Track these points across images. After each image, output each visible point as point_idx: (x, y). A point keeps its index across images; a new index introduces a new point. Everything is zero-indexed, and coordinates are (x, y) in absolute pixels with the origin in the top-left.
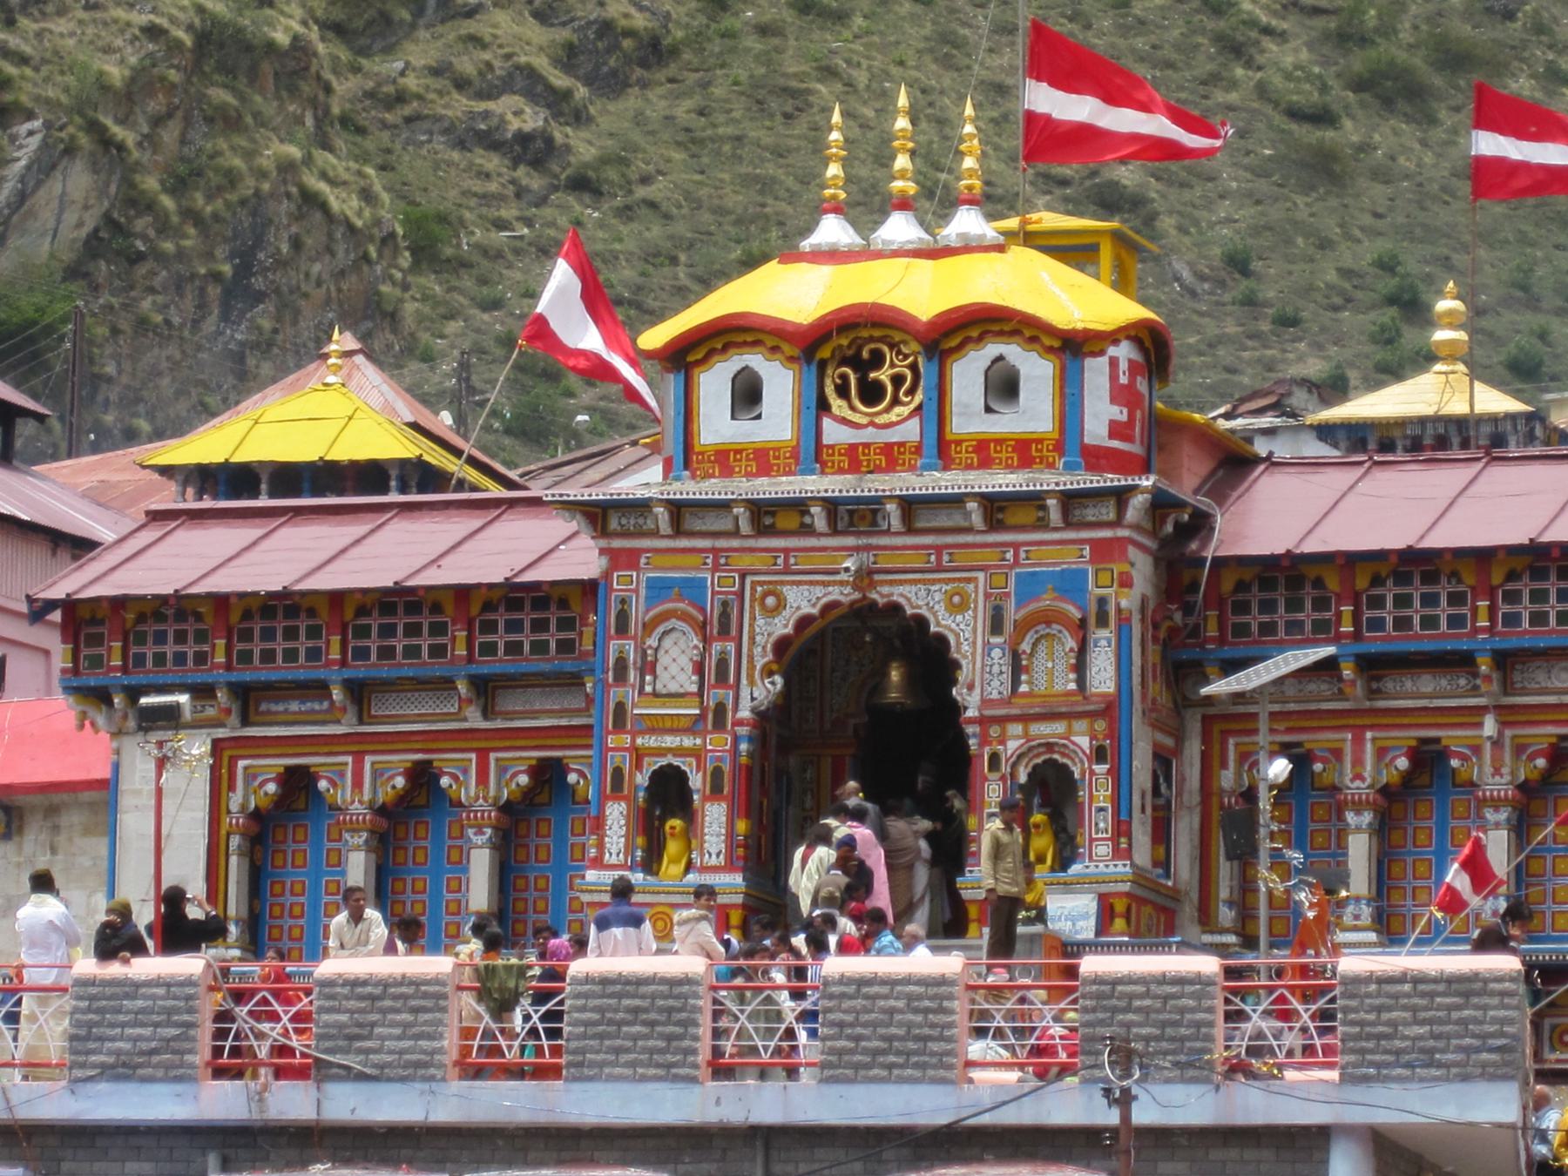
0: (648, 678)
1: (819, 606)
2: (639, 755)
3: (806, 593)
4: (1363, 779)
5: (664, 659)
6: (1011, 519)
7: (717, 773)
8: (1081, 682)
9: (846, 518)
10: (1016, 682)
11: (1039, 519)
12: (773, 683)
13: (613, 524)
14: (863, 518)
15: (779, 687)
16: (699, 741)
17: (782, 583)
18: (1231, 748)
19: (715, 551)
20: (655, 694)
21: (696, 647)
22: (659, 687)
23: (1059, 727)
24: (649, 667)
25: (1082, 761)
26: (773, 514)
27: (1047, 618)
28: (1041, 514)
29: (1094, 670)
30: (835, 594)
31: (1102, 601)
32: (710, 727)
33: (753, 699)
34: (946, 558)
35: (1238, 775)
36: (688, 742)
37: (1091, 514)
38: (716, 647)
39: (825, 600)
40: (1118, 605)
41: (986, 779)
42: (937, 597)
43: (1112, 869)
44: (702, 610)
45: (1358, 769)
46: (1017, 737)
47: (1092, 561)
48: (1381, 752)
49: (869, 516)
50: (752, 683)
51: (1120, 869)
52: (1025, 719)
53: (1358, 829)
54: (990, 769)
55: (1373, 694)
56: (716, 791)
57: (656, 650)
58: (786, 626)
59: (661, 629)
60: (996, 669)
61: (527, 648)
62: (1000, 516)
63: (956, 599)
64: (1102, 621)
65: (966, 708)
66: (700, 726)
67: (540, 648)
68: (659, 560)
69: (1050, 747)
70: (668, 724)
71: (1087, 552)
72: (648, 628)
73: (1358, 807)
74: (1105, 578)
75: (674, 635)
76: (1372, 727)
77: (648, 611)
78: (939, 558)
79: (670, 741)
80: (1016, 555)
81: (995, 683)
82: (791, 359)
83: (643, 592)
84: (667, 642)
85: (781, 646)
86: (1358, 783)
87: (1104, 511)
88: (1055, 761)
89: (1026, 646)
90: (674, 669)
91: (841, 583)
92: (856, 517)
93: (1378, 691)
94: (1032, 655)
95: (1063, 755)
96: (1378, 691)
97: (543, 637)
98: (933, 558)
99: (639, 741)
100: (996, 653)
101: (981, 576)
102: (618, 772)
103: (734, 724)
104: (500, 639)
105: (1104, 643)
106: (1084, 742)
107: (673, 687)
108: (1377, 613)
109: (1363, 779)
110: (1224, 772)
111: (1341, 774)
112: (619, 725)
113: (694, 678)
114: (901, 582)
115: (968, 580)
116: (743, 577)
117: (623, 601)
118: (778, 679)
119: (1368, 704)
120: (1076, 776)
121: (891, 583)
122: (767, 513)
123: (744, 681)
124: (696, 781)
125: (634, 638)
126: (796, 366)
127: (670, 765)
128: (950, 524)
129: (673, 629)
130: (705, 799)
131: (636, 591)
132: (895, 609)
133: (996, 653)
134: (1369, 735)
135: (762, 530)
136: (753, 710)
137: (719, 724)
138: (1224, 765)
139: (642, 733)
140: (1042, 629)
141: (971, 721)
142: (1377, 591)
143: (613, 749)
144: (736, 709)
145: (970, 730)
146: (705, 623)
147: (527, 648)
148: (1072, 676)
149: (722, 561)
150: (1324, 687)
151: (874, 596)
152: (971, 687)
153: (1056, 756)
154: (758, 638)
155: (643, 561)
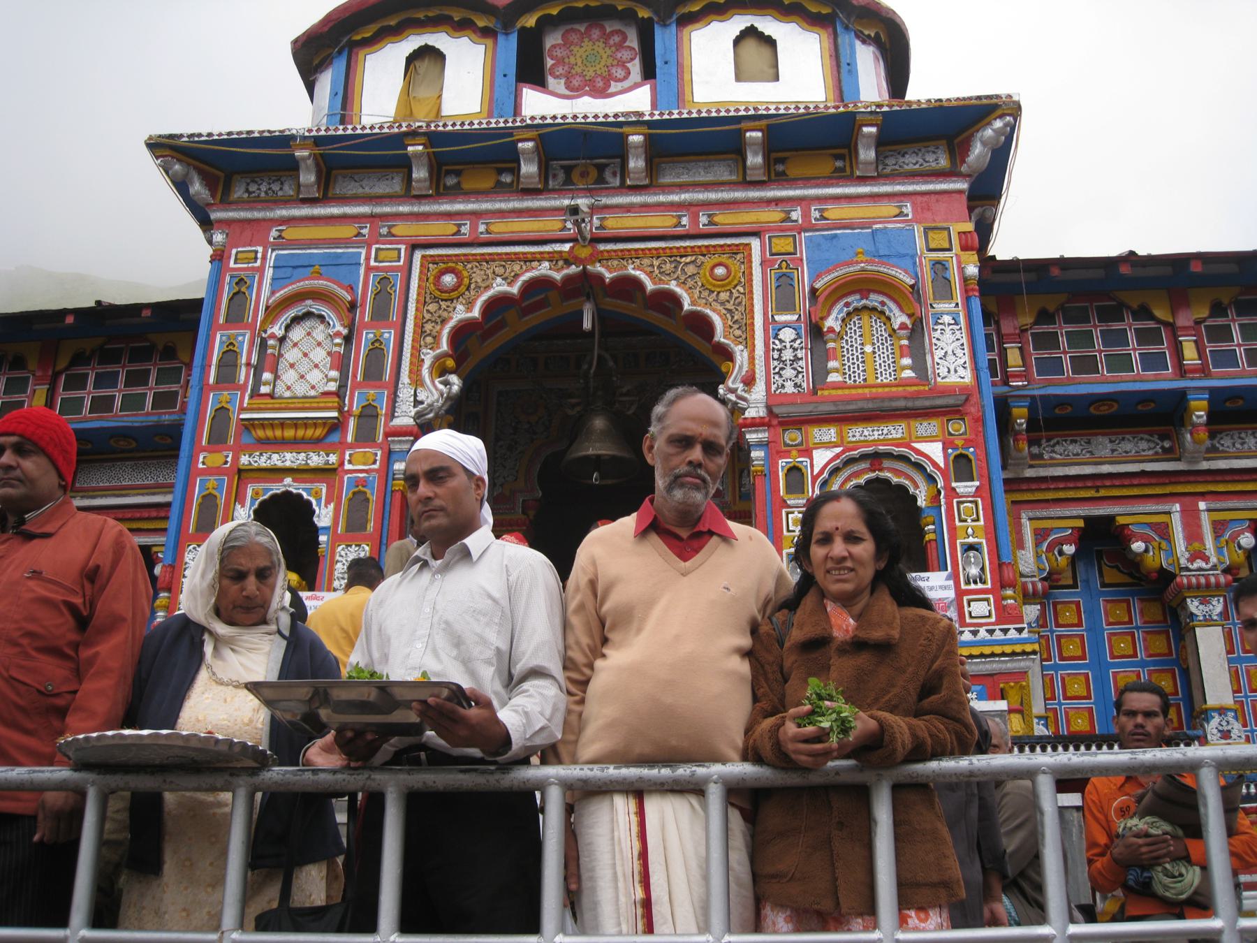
0: (267, 376)
1: (519, 284)
2: (243, 475)
3: (500, 270)
4: (1206, 559)
5: (291, 355)
6: (793, 172)
7: (359, 500)
8: (920, 366)
9: (561, 176)
10: (820, 372)
11: (837, 170)
12: (446, 383)
13: (238, 192)
14: (584, 175)
15: (455, 388)
16: (333, 458)
17: (467, 259)
18: (1025, 521)
19: (372, 217)
20: (271, 396)
21: (338, 334)
22: (280, 389)
23: (895, 431)
24: (268, 360)
25: (931, 479)
26: (458, 173)
27: (863, 285)
28: (839, 164)
29: (939, 354)
30: (544, 269)
31: (940, 266)
32: (350, 439)
33: (417, 403)
34: (703, 219)
35: (1038, 556)
36: (316, 460)
37: (911, 162)
38: (367, 336)
39: (526, 276)
40: (961, 270)
41: (784, 504)
42: (691, 270)
43: (998, 635)
44: (351, 289)
45: (1196, 545)
46: (828, 445)
47: (916, 220)
48: (1219, 528)
49: (594, 174)
50: (417, 381)
51: (1012, 634)
52: (843, 418)
53: (1208, 622)
54: (790, 489)
55: (1213, 453)
56: (354, 528)
57: (282, 340)
58: (469, 309)
59: (292, 313)
60: (788, 355)
61: (118, 403)
62: (780, 168)
63: (720, 271)
64: (944, 292)
65: (743, 410)
66: (335, 438)
67: (133, 403)
68: (291, 233)
69: (876, 458)
70: (289, 433)
71: (908, 209)
72: (273, 312)
73: (1206, 591)
74: (938, 239)
75: (308, 324)
76: (1203, 495)
77: (273, 293)
78: (695, 219)
79: (289, 459)
80: (806, 215)
81: (789, 373)
82: (487, 33)
83: (269, 273)
84: (297, 334)
85: (462, 334)
86: (1199, 563)
87: (930, 157)
88: (887, 482)
89: (832, 322)
90: (304, 367)
91: (552, 258)
92: (575, 176)
93: (1213, 449)
94: (840, 336)
95: (897, 472)
96: (1213, 449)
97: (139, 390)
98: (685, 221)
99: (244, 460)
100: (787, 334)
101: (755, 244)
102: (209, 501)
103: (387, 435)
104: (88, 395)
105: (947, 319)
106: (935, 451)
107: (301, 389)
108: (1224, 346)
109: (1206, 559)
110: (1020, 553)
111: (1171, 551)
112: (218, 439)
113: (334, 374)
114: (637, 255)
115: (734, 251)
116: (414, 247)
117: (241, 281)
118: (454, 379)
119: (1205, 465)
120: (921, 502)
121: (624, 256)
122: (448, 173)
123: (405, 378)
124: (324, 517)
125: (252, 327)
126: (490, 42)
127: (287, 494)
128: (709, 178)
129: (308, 315)
130: (336, 540)
131: (261, 270)
132: (629, 286)
133: (787, 334)
134: (1202, 505)
135: (439, 190)
136: (418, 416)
137: (365, 437)
138: (1020, 545)
139: (249, 449)
140: (855, 301)
141: (755, 424)
142: (1220, 321)
143: (210, 471)
144: (391, 414)
145: (752, 437)
146: (353, 306)
147: (118, 403)
148: (907, 361)
149: (384, 231)
150: (1143, 445)
151: (599, 268)
152: (749, 381)
153: (888, 475)
154: (428, 327)
155: (274, 233)
